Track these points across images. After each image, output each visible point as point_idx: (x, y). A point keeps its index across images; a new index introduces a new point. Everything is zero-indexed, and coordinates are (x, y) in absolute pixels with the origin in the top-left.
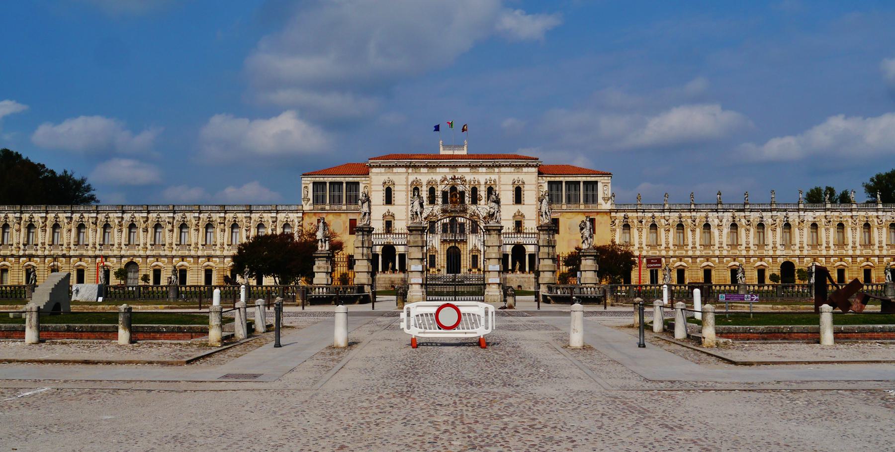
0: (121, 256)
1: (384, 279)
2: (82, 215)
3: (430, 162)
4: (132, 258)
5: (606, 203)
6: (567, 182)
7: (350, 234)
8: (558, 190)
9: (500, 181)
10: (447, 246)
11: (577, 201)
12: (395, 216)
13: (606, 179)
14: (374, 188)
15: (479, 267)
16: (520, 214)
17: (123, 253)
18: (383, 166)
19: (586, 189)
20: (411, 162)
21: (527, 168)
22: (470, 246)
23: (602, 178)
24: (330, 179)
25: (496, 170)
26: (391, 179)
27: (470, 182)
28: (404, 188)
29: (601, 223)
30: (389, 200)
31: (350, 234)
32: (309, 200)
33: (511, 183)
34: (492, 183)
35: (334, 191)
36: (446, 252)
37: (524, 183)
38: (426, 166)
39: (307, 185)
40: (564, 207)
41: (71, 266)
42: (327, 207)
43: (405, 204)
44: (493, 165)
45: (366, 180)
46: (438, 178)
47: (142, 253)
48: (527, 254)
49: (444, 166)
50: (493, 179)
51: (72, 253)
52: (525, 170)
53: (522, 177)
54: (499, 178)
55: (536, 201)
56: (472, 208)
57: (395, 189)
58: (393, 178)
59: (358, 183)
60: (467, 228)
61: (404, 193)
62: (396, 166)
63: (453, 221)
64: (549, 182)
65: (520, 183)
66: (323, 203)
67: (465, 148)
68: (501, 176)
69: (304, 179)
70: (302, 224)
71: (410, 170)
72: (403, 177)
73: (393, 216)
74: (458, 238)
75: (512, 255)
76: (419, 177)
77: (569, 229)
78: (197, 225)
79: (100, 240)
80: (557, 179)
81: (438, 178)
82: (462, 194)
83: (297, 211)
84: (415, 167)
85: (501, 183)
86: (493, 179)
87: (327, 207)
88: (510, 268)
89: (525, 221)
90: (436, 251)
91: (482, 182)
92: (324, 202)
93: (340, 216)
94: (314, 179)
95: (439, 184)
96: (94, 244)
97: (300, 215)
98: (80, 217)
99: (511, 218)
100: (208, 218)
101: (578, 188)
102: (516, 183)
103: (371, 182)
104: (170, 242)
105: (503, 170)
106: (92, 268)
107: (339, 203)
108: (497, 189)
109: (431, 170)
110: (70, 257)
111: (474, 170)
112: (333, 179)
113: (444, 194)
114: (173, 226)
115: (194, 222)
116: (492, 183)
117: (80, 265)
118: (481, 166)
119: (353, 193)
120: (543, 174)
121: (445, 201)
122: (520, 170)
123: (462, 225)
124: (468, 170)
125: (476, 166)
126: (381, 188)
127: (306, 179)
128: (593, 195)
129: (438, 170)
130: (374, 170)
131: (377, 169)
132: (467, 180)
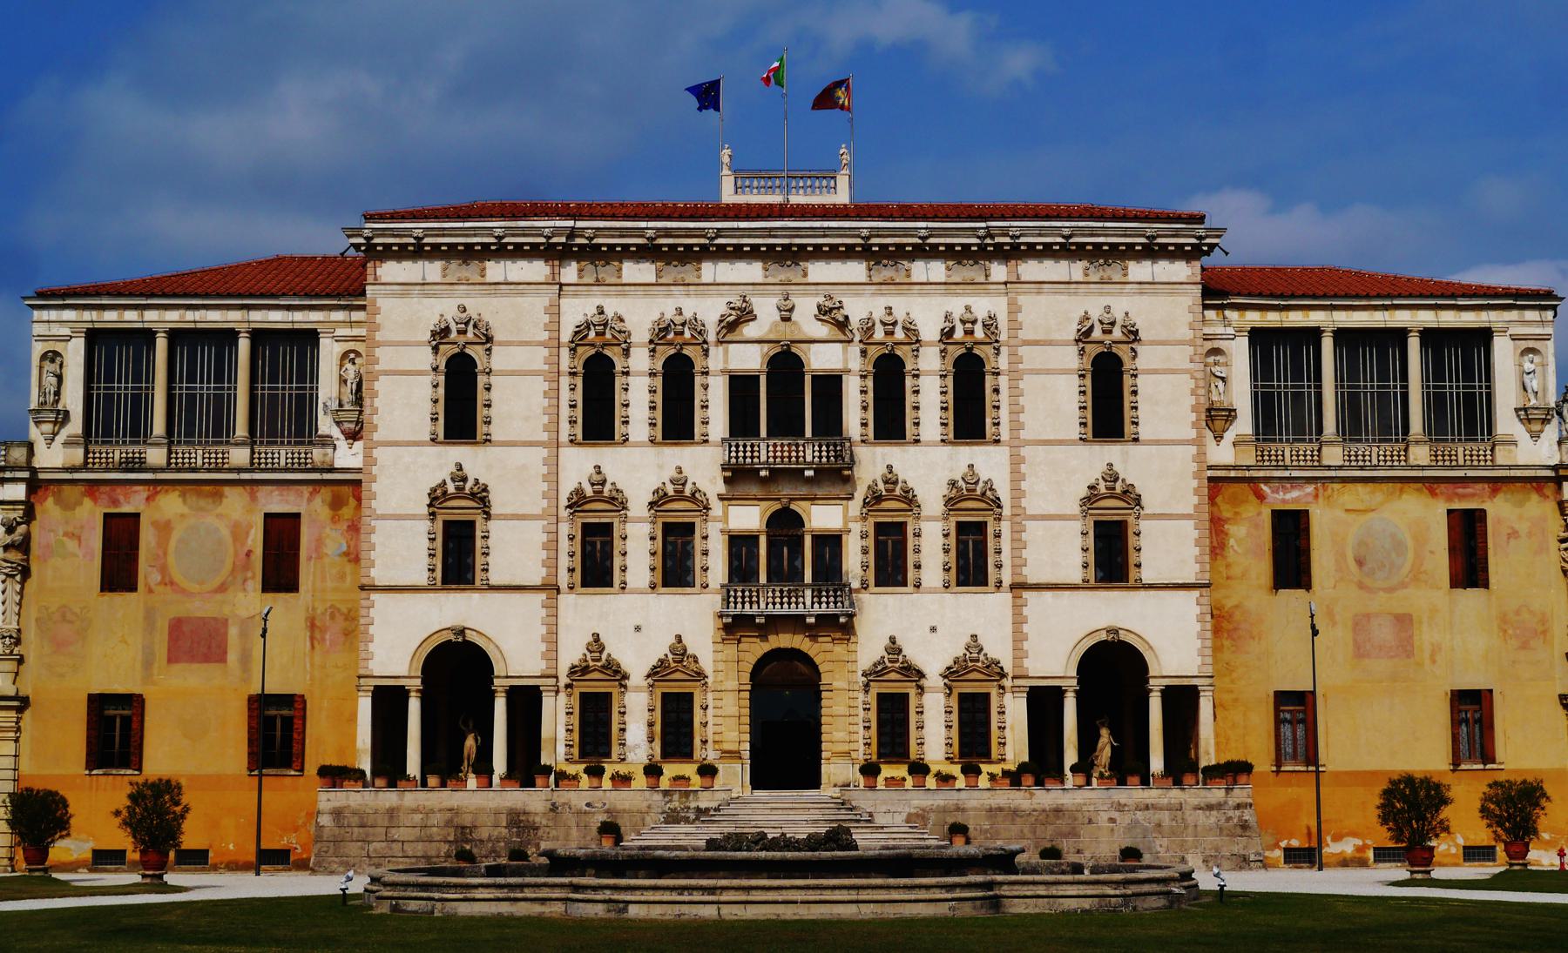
1: (418, 818)
3: (668, 233)
5: (1535, 436)
6: (1341, 335)
8: (1298, 376)
9: (1015, 325)
10: (756, 649)
11: (1392, 427)
12: (497, 505)
13: (1530, 321)
14: (386, 358)
15: (913, 756)
16: (1119, 487)
18: (436, 247)
19: (1435, 371)
20: (572, 233)
21: (1147, 264)
22: (868, 648)
23: (1514, 315)
24: (173, 316)
25: (999, 271)
26: (472, 312)
27: (868, 329)
28: (537, 358)
29: (1513, 534)
32: (63, 418)
33: (1072, 334)
34: (979, 333)
35: (192, 379)
36: (746, 678)
37: (1133, 335)
38: (648, 252)
39: (58, 347)
40: (1333, 455)
42: (156, 456)
43: (544, 437)
44: (982, 247)
45: (351, 324)
46: (710, 310)
48: (1156, 685)
49: (738, 247)
50: (981, 313)
52: (1140, 270)
53: (1123, 305)
54: (1014, 310)
55: (1195, 425)
56: (873, 461)
57: (495, 366)
58: (482, 306)
59: (309, 338)
60: (855, 560)
61: (540, 385)
62: (501, 251)
63: (785, 524)
64: (1260, 339)
65: (1117, 333)
66: (135, 432)
67: (843, 181)
68: (1022, 299)
69: (45, 315)
70: (27, 537)
71: (570, 272)
72: (535, 306)
73: (481, 497)
74: (808, 605)
75: (1079, 695)
76: (613, 306)
77: (1360, 563)
80: (1295, 319)
81: (710, 310)
82: (830, 385)
84: (593, 254)
85: (1022, 335)
86: (981, 313)
87: (156, 456)
88: (1071, 757)
89: (1144, 525)
90: (700, 675)
91: (930, 331)
92: (138, 430)
93: (219, 497)
94: (94, 315)
95: (711, 337)
97: (18, 492)
99: (1075, 509)
101: (1393, 365)
102: (1097, 334)
103: (373, 327)
105: (1031, 269)
108: (1003, 362)
109: (673, 273)
111: (886, 273)
112: (190, 315)
113: (741, 386)
116: (979, 333)
118: (925, 251)
119: (287, 389)
120: (1224, 294)
121: (742, 423)
122: (1114, 272)
123: (830, 543)
124: (855, 270)
125: (899, 254)
126: (424, 358)
127: (53, 315)
128: (1470, 399)
129: (710, 271)
130: (390, 271)
131: (407, 264)
132: (855, 323)
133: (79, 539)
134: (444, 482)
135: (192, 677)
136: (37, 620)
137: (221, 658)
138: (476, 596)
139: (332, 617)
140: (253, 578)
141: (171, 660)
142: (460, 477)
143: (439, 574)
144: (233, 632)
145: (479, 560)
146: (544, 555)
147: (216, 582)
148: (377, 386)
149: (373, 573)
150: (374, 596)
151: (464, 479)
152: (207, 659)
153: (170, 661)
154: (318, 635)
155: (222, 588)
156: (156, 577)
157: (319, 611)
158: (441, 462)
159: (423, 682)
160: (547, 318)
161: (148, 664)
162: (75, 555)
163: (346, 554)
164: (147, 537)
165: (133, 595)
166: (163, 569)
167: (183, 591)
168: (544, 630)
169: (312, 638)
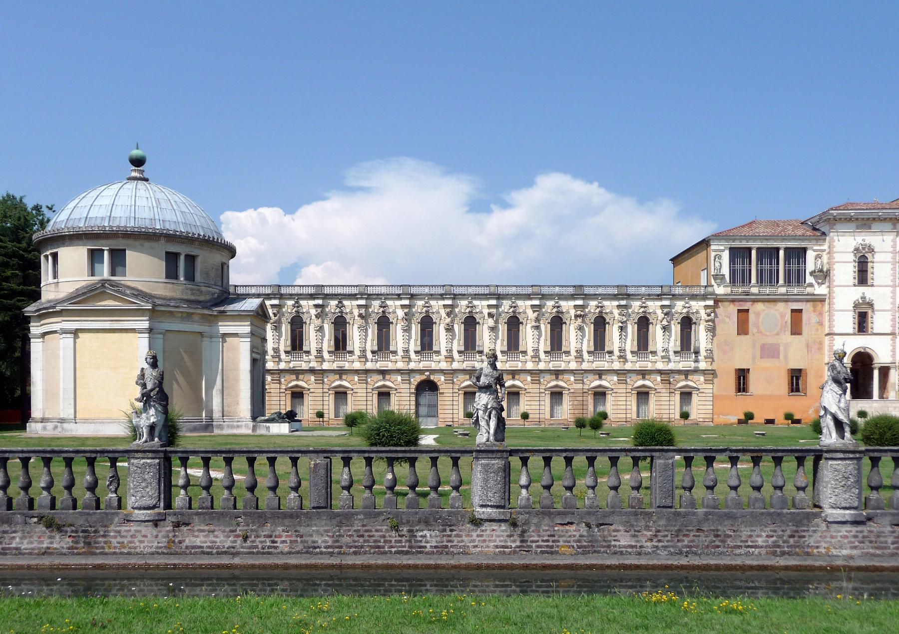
0: (408, 370)
2: (297, 302)
4: (427, 373)
12: (876, 307)
14: (837, 257)
17: (412, 366)
30: (863, 276)
41: (326, 386)
47: (444, 365)
51: (326, 366)
61: (890, 266)
73: (870, 305)
78: (537, 320)
79: (372, 344)
83: (704, 297)
96: (364, 351)
97: (711, 303)
98: (337, 306)
100: (381, 307)
104: (492, 347)
106: (275, 395)
110: (323, 372)
114: (496, 322)
115: (531, 315)
117: (340, 386)
133: (729, 318)
134: (858, 300)
135: (768, 363)
136: (717, 344)
137: (778, 357)
139: (814, 343)
141: (761, 358)
142: (863, 298)
143: (857, 330)
144: (782, 348)
145: (870, 325)
146: (891, 323)
147: (776, 332)
148: (834, 266)
149: (834, 329)
150: (835, 337)
151: (865, 298)
152: (773, 357)
153: (761, 358)
154: (810, 349)
155: (778, 334)
156: (755, 330)
157: (810, 341)
158: (859, 292)
159: (852, 364)
160: (892, 243)
161: (754, 359)
162: (728, 323)
163: (818, 323)
165: (748, 336)
166: (758, 328)
168: (891, 348)
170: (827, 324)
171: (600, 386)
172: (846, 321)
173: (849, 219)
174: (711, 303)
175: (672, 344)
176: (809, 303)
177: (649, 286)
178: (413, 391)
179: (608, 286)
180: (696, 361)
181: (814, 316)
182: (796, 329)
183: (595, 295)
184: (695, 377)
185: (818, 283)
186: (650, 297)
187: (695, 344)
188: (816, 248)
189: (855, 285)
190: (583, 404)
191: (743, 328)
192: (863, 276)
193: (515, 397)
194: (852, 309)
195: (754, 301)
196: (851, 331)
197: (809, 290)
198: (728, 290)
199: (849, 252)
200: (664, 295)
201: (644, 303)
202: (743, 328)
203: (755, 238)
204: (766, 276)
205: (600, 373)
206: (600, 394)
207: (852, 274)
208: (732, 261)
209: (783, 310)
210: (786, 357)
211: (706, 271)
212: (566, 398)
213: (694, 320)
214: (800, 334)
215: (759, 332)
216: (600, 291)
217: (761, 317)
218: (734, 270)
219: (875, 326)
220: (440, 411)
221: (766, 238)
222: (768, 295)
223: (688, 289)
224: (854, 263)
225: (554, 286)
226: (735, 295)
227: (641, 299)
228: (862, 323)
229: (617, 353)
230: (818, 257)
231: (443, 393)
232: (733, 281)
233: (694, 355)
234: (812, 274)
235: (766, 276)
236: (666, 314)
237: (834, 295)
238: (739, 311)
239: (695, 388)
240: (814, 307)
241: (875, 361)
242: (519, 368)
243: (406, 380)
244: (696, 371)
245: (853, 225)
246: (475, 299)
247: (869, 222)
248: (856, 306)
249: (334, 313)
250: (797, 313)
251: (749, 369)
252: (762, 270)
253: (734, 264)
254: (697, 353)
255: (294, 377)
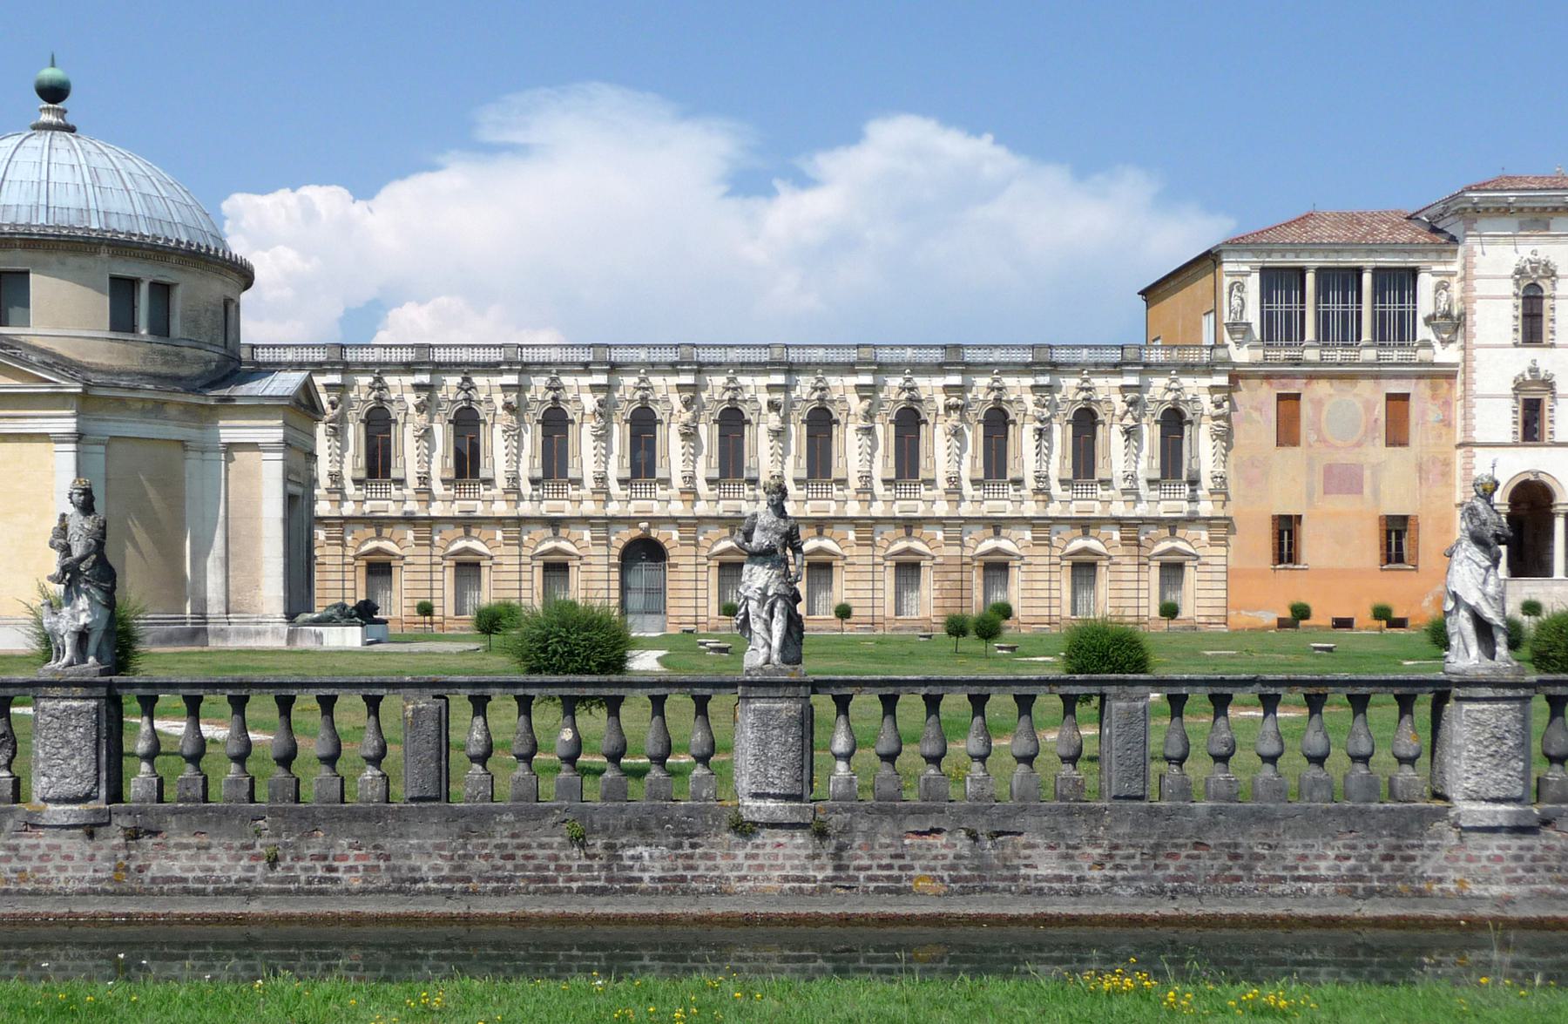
4: (644, 525)
7: (1388, 445)
12: (1559, 390)
14: (1480, 287)
17: (613, 509)
30: (1532, 328)
31: (1388, 445)
41: (438, 552)
47: (678, 508)
51: (437, 510)
59: (1414, 273)
73: (1548, 385)
78: (869, 415)
83: (1209, 369)
96: (514, 479)
97: (1223, 380)
98: (460, 387)
100: (549, 388)
104: (777, 471)
107: (1402, 338)
114: (785, 420)
115: (857, 405)
117: (467, 551)
134: (1522, 375)
136: (1235, 465)
137: (1360, 491)
138: (1545, 449)
140: (1380, 437)
142: (1534, 370)
143: (1520, 435)
144: (1367, 473)
145: (1547, 426)
148: (1475, 306)
149: (1475, 434)
150: (1475, 450)
151: (1537, 370)
152: (1349, 491)
153: (1325, 493)
154: (1424, 475)
155: (1359, 444)
159: (1510, 506)
161: (1310, 496)
163: (1442, 421)
164: (1306, 408)
165: (1297, 449)
166: (1319, 431)
167: (1332, 446)
169: (1420, 478)
170: (1459, 423)
171: (997, 551)
172: (1499, 419)
173: (1504, 210)
174: (1223, 380)
175: (1143, 464)
176: (1423, 383)
177: (1096, 347)
178: (615, 560)
179: (1013, 347)
180: (1193, 499)
181: (1433, 407)
182: (1397, 435)
183: (987, 364)
184: (1191, 533)
185: (1442, 341)
186: (1100, 369)
187: (1190, 465)
188: (1436, 268)
189: (1516, 345)
190: (962, 589)
191: (1288, 433)
192: (1532, 328)
193: (823, 573)
194: (1511, 392)
195: (1311, 377)
196: (1509, 439)
197: (1423, 354)
198: (1258, 355)
199: (1505, 277)
200: (1128, 364)
201: (1086, 381)
202: (1288, 433)
203: (1312, 248)
204: (1335, 326)
205: (996, 525)
206: (996, 568)
207: (1511, 321)
208: (1266, 295)
209: (1370, 397)
210: (1376, 492)
211: (1212, 315)
212: (927, 576)
213: (1189, 416)
214: (1403, 443)
215: (1322, 440)
216: (997, 356)
217: (1326, 408)
218: (1270, 314)
219: (1557, 428)
220: (670, 602)
221: (1337, 249)
222: (1339, 365)
223: (1175, 353)
224: (1514, 300)
225: (903, 347)
226: (1272, 365)
227: (1080, 372)
228: (1532, 423)
229: (1030, 483)
230: (1442, 287)
231: (676, 565)
232: (1268, 335)
233: (1188, 488)
234: (1429, 320)
235: (1335, 326)
236: (1131, 404)
237: (1475, 364)
238: (1280, 397)
239: (1190, 554)
240: (1434, 388)
241: (1558, 500)
242: (832, 514)
243: (602, 538)
244: (1192, 520)
245: (1513, 222)
246: (742, 372)
247: (1545, 215)
248: (1519, 386)
249: (454, 402)
250: (1398, 401)
251: (1299, 517)
252: (1326, 314)
253: (1270, 301)
254: (1194, 482)
255: (372, 532)
